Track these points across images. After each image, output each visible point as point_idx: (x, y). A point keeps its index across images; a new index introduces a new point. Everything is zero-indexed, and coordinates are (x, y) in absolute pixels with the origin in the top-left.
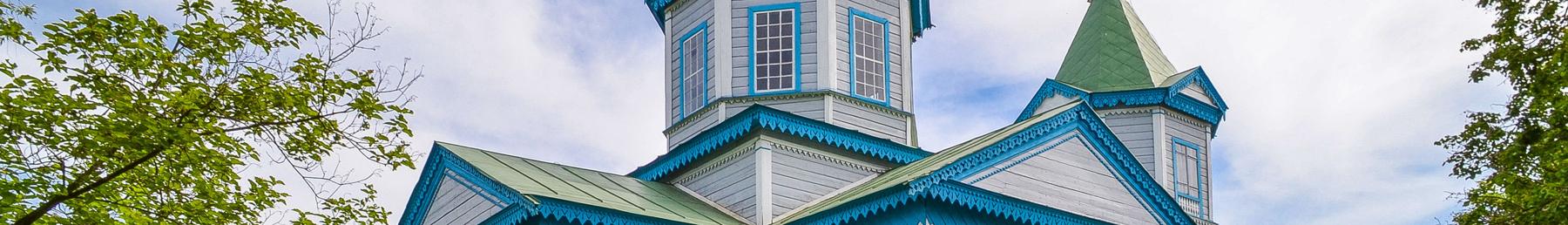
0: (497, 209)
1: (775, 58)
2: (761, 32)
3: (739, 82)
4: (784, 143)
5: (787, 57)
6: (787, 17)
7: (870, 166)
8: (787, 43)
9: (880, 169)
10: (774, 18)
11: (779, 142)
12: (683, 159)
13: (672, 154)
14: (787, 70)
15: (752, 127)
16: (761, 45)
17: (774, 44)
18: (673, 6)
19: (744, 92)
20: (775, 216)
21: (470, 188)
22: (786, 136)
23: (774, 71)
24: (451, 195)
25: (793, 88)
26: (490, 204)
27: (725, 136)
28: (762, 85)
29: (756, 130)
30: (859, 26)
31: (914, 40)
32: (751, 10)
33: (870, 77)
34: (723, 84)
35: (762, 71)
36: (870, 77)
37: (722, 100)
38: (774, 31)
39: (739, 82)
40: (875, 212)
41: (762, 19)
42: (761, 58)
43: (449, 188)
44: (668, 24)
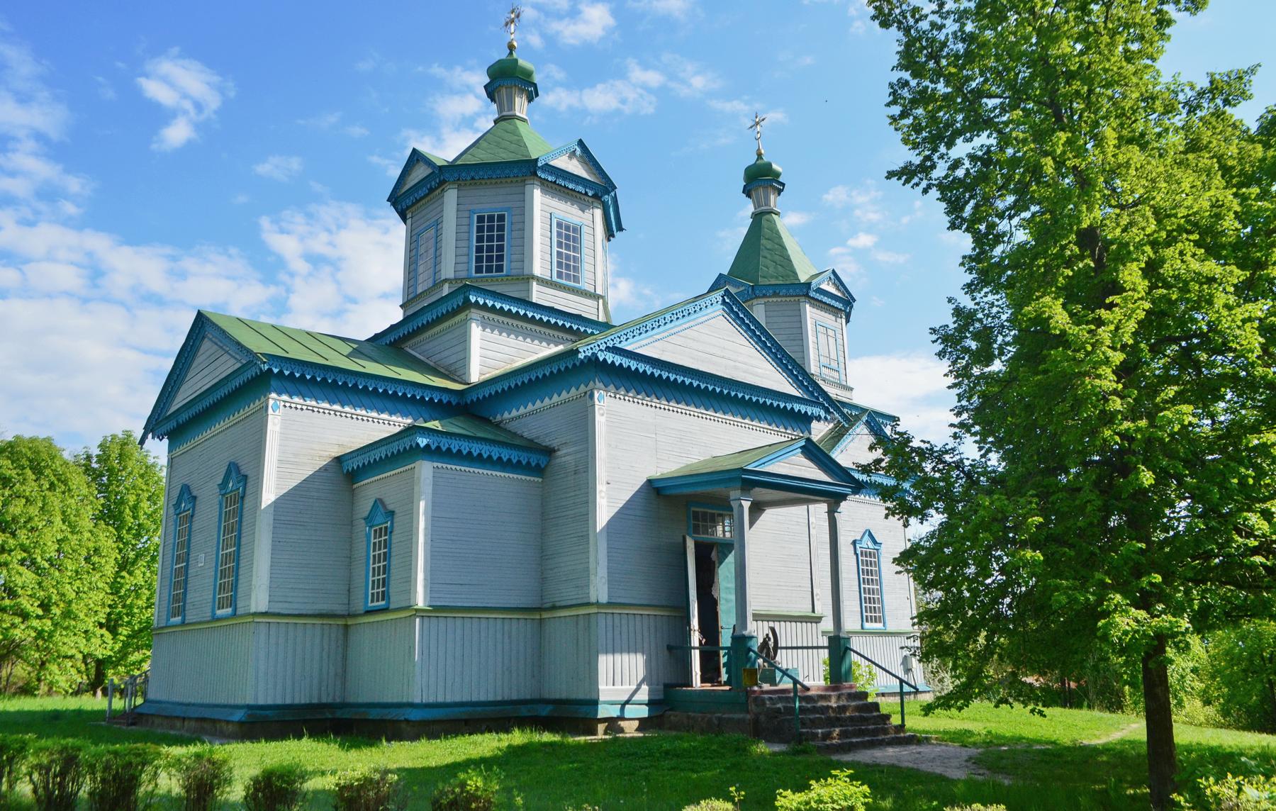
0: (238, 365)
1: (490, 249)
2: (480, 229)
3: (460, 267)
4: (492, 316)
5: (500, 248)
6: (501, 218)
7: (566, 336)
8: (501, 238)
9: (574, 338)
10: (491, 218)
11: (487, 315)
12: (410, 327)
13: (406, 320)
14: (500, 258)
15: (463, 303)
16: (480, 239)
17: (490, 239)
18: (413, 209)
19: (463, 274)
20: (481, 374)
21: (221, 347)
22: (493, 309)
23: (490, 259)
24: (208, 353)
25: (505, 273)
26: (233, 361)
27: (443, 309)
28: (479, 270)
29: (467, 305)
30: (559, 225)
31: (609, 240)
32: (472, 212)
33: (568, 267)
34: (448, 271)
35: (479, 259)
36: (568, 267)
37: (446, 280)
38: (490, 229)
39: (460, 267)
40: (555, 372)
41: (481, 219)
42: (479, 249)
43: (207, 347)
44: (409, 221)
